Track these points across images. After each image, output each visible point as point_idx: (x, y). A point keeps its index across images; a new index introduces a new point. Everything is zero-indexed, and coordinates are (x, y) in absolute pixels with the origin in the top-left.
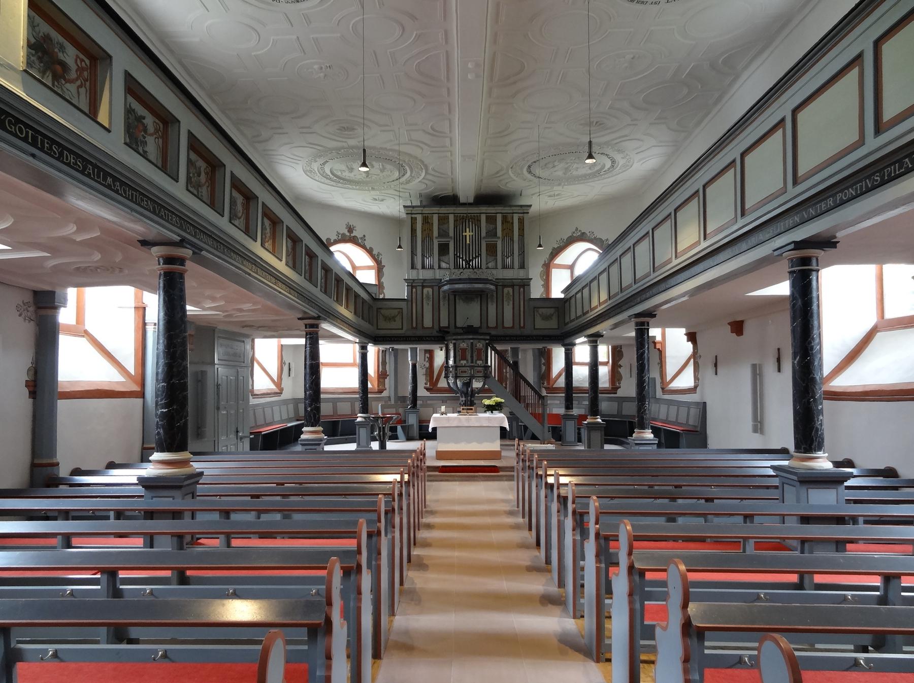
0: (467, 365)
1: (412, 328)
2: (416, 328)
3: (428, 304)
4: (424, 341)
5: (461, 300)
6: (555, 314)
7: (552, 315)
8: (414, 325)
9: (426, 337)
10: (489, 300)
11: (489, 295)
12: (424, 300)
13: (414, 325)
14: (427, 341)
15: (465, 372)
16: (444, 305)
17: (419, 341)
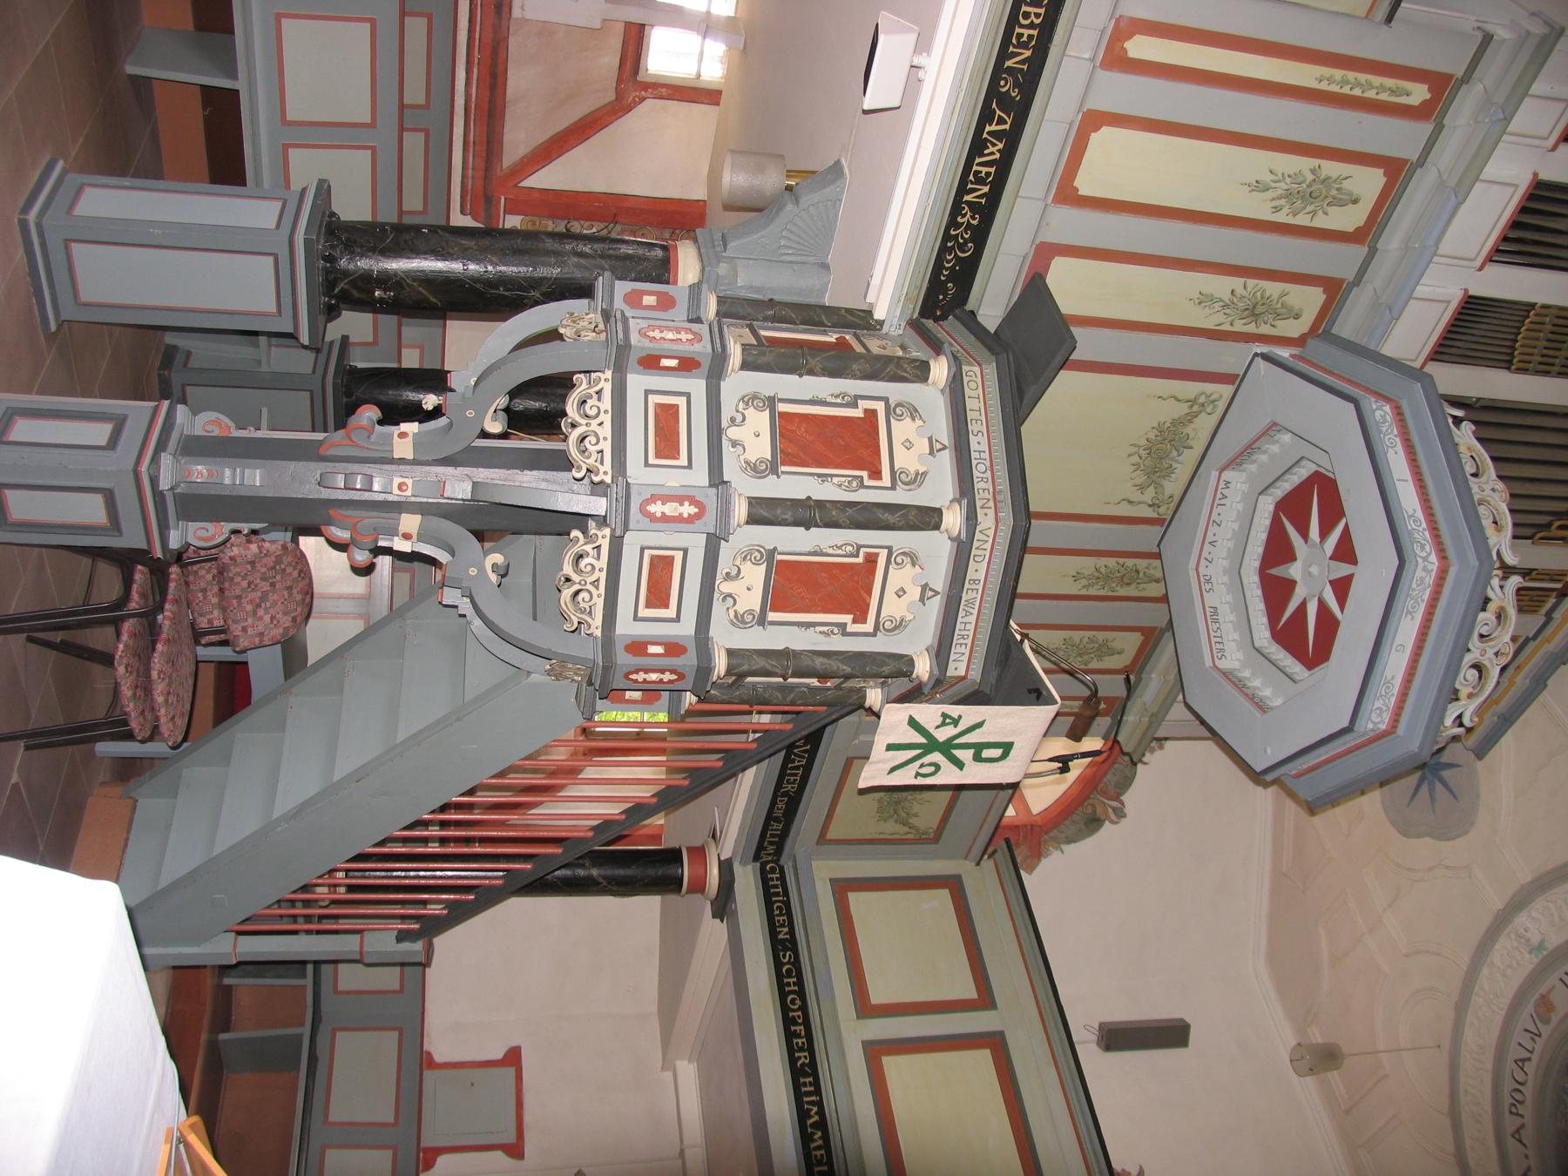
0: (718, 610)
1: (1126, 28)
2: (1116, 59)
3: (1259, 187)
4: (986, 116)
5: (1183, 409)
6: (906, 829)
7: (905, 823)
8: (1140, 47)
9: (1012, 140)
10: (1111, 562)
11: (1142, 563)
12: (1303, 164)
13: (1140, 47)
14: (978, 146)
15: (658, 596)
16: (1204, 300)
17: (998, 71)
